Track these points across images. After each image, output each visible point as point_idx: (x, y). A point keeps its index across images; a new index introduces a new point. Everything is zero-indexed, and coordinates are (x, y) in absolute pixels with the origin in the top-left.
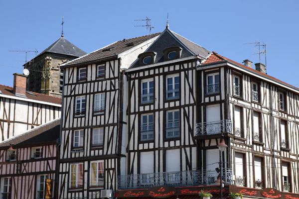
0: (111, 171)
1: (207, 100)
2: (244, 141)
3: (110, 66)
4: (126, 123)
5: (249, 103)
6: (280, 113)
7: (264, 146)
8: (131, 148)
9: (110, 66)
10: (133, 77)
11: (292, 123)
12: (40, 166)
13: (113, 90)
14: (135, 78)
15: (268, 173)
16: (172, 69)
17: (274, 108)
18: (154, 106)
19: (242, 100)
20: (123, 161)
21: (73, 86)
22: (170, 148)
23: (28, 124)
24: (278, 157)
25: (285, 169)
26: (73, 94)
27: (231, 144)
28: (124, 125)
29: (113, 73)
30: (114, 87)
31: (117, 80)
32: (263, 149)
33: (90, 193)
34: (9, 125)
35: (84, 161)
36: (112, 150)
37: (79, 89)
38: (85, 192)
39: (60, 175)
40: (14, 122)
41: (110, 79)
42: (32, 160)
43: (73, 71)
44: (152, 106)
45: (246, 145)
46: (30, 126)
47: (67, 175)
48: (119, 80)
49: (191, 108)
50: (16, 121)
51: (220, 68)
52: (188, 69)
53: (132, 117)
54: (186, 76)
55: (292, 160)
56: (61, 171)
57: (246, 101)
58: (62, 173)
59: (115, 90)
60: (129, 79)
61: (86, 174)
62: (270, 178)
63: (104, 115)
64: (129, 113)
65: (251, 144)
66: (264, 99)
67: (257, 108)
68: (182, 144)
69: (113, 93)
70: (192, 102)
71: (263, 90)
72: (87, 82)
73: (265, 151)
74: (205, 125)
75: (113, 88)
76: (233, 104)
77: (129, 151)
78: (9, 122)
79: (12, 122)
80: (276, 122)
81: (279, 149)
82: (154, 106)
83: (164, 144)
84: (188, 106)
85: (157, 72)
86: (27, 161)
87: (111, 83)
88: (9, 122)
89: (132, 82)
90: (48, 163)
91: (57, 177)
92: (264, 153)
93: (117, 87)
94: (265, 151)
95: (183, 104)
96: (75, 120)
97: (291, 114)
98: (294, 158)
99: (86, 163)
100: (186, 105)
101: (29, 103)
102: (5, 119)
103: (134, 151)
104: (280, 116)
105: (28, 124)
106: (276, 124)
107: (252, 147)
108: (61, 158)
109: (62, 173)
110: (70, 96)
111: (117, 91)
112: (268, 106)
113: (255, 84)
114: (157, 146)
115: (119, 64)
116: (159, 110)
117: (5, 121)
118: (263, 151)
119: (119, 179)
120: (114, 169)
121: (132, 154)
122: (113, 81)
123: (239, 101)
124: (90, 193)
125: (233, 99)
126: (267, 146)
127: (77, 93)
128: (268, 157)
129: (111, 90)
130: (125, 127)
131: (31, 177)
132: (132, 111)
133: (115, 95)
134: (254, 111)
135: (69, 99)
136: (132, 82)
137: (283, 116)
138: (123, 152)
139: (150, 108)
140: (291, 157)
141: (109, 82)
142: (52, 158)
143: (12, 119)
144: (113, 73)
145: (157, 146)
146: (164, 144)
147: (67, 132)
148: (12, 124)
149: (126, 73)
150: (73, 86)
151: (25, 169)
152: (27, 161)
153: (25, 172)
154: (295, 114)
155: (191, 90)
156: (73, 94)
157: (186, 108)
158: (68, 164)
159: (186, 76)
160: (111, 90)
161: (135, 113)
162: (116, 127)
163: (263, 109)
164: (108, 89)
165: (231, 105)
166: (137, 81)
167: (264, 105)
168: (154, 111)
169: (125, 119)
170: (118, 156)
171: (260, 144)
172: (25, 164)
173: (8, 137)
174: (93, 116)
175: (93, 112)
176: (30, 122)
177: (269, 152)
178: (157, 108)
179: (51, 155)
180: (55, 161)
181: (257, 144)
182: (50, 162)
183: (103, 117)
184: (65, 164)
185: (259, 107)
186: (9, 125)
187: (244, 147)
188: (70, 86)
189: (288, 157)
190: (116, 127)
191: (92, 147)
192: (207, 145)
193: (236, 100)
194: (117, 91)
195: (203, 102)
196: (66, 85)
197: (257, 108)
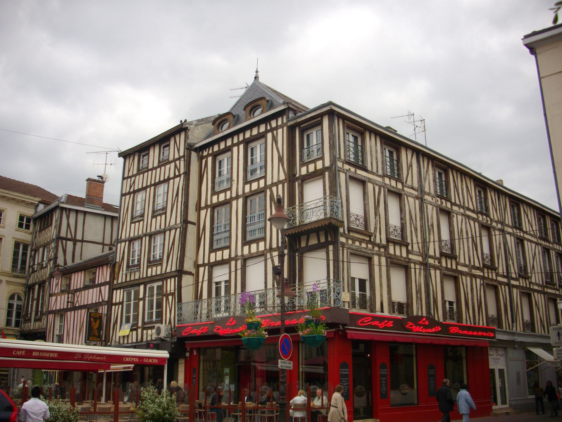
0: (170, 297)
1: (304, 171)
2: (370, 237)
3: (175, 142)
4: (194, 224)
5: (380, 176)
6: (439, 199)
7: (410, 248)
8: (200, 262)
9: (175, 142)
10: (205, 153)
11: (460, 217)
12: (91, 296)
14: (209, 155)
15: (418, 291)
16: (255, 132)
17: (427, 190)
18: (231, 193)
19: (365, 169)
20: (187, 280)
22: (252, 257)
23: (103, 244)
24: (435, 268)
25: (449, 287)
26: (132, 190)
27: (342, 240)
28: (190, 227)
29: (179, 150)
30: (179, 171)
32: (408, 252)
33: (145, 332)
34: (75, 245)
35: (139, 285)
36: (172, 266)
37: (139, 181)
38: (140, 331)
39: (113, 307)
40: (82, 241)
41: (175, 160)
42: (86, 288)
43: (134, 159)
44: (228, 193)
45: (374, 244)
46: (107, 248)
47: (121, 306)
49: (280, 186)
50: (85, 239)
52: (277, 128)
53: (203, 212)
54: (275, 139)
55: (462, 273)
56: (114, 301)
57: (373, 173)
58: (116, 304)
60: (201, 158)
61: (141, 303)
62: (421, 301)
63: (165, 213)
64: (199, 208)
65: (384, 242)
66: (408, 174)
67: (395, 186)
68: (268, 247)
69: (177, 180)
70: (282, 177)
71: (406, 157)
72: (148, 171)
73: (411, 256)
74: (302, 213)
75: (177, 174)
76: (346, 174)
77: (197, 266)
78: (75, 241)
79: (79, 241)
80: (431, 211)
81: (438, 255)
82: (231, 193)
83: (242, 251)
84: (276, 184)
85: (235, 141)
86: (79, 290)
88: (75, 241)
89: (204, 161)
91: (110, 310)
92: (410, 259)
94: (411, 256)
95: (269, 182)
96: (133, 225)
97: (458, 202)
98: (465, 269)
99: (142, 287)
100: (273, 184)
101: (105, 216)
102: (69, 236)
103: (204, 265)
104: (439, 203)
105: (103, 244)
106: (432, 214)
107: (386, 248)
109: (116, 304)
111: (182, 176)
112: (416, 185)
113: (392, 150)
114: (233, 255)
115: (186, 137)
116: (237, 197)
117: (70, 240)
118: (407, 255)
119: (180, 309)
120: (173, 294)
121: (201, 269)
123: (359, 172)
124: (145, 332)
125: (347, 167)
126: (416, 248)
127: (136, 188)
128: (417, 266)
130: (192, 230)
131: (83, 311)
132: (203, 205)
133: (180, 182)
134: (389, 191)
135: (128, 197)
137: (444, 204)
138: (188, 266)
139: (226, 196)
140: (460, 268)
142: (104, 284)
143: (79, 237)
145: (233, 255)
146: (242, 251)
147: (123, 244)
148: (79, 244)
149: (197, 148)
150: (133, 179)
151: (77, 301)
152: (79, 290)
153: (77, 305)
154: (464, 203)
155: (281, 159)
159: (275, 139)
161: (206, 207)
162: (178, 230)
163: (406, 189)
164: (172, 175)
165: (342, 176)
166: (210, 159)
167: (409, 183)
168: (232, 199)
169: (192, 217)
170: (180, 273)
171: (403, 243)
172: (78, 293)
173: (73, 261)
174: (153, 217)
175: (154, 212)
176: (107, 241)
177: (420, 259)
178: (234, 195)
181: (395, 243)
183: (163, 216)
184: (119, 291)
185: (400, 186)
186: (75, 245)
187: (370, 246)
189: (454, 267)
190: (178, 230)
191: (151, 263)
192: (303, 244)
193: (353, 169)
195: (298, 175)
197: (395, 186)
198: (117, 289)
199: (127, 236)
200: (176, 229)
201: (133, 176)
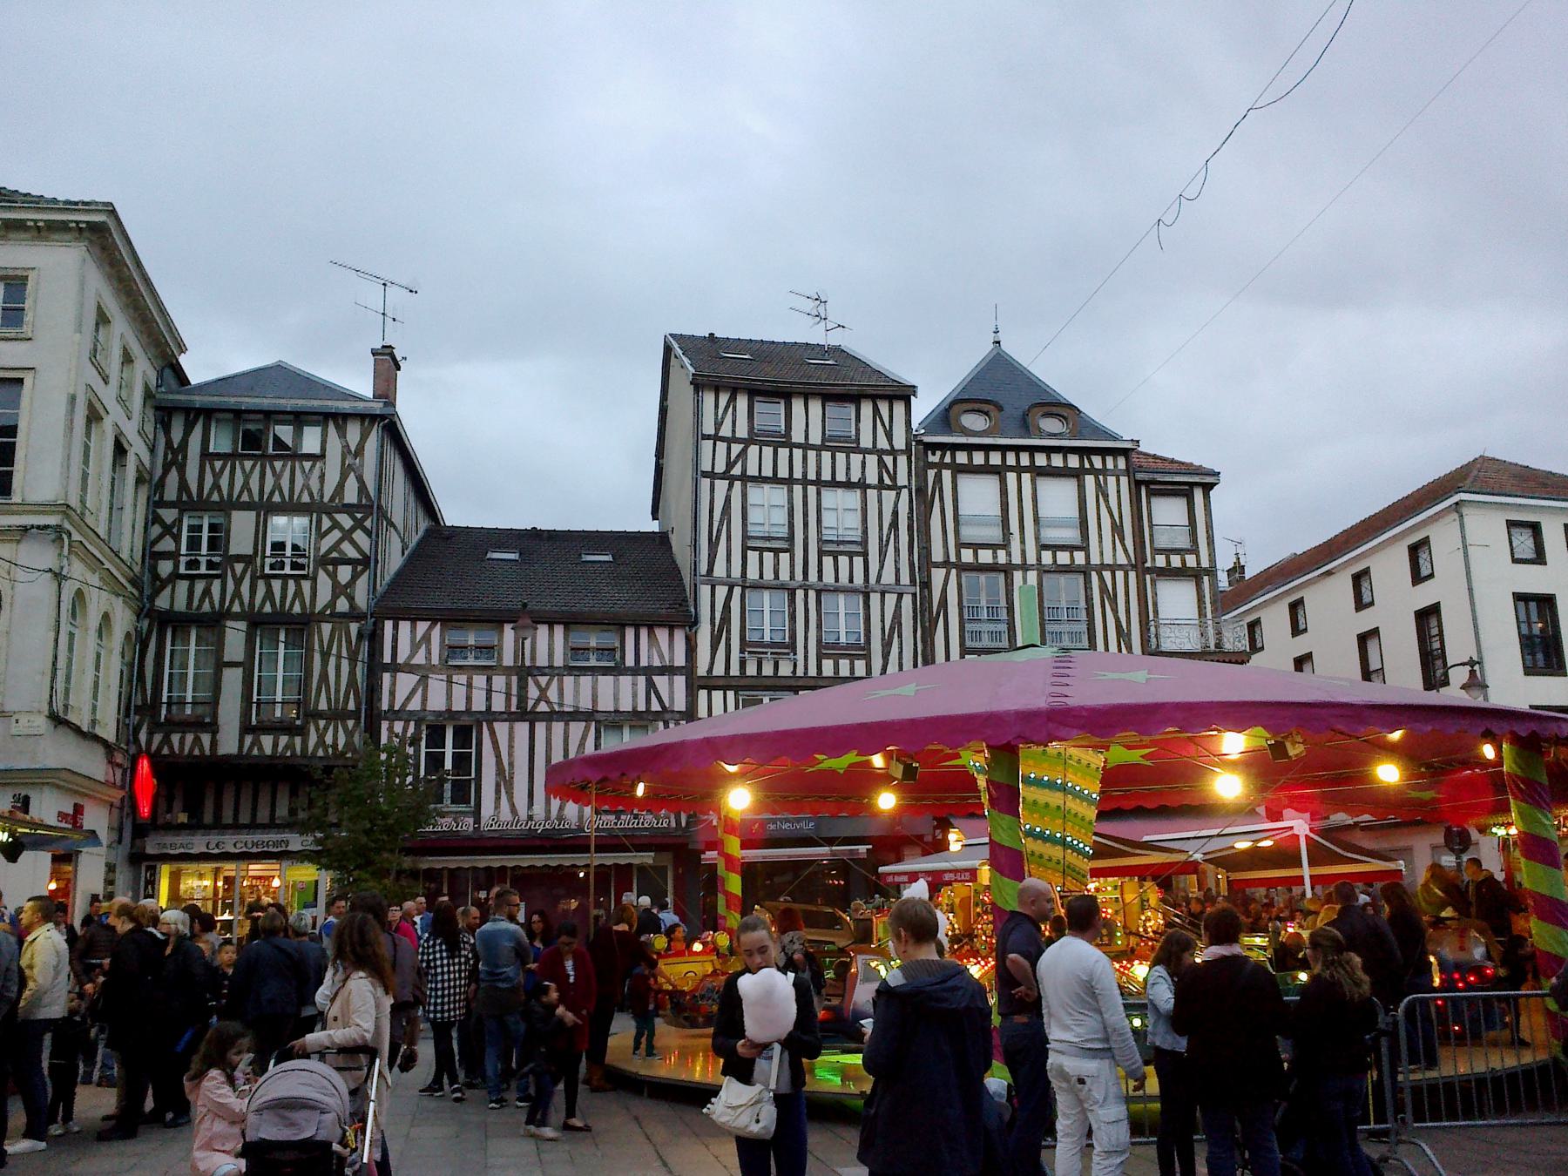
1: (1161, 561)
3: (876, 412)
13: (889, 488)
14: (941, 466)
18: (1009, 554)
21: (736, 449)
29: (889, 435)
30: (894, 478)
31: (902, 460)
48: (909, 459)
49: (1120, 575)
51: (1192, 485)
52: (1104, 471)
54: (1102, 491)
59: (894, 487)
75: (887, 481)
87: (881, 464)
90: (651, 685)
93: (902, 479)
95: (1095, 560)
108: (702, 670)
110: (725, 476)
111: (905, 492)
122: (888, 460)
129: (881, 486)
136: (931, 473)
141: (872, 460)
142: (669, 670)
144: (889, 435)
150: (736, 449)
155: (1117, 529)
156: (737, 471)
157: (1107, 575)
158: (731, 694)
159: (1102, 491)
160: (881, 486)
161: (946, 564)
179: (661, 657)
180: (680, 681)
182: (661, 682)
183: (858, 561)
188: (721, 446)
194: (905, 492)
196: (708, 437)
198: (710, 689)
199: (736, 572)
200: (900, 596)
201: (733, 439)
